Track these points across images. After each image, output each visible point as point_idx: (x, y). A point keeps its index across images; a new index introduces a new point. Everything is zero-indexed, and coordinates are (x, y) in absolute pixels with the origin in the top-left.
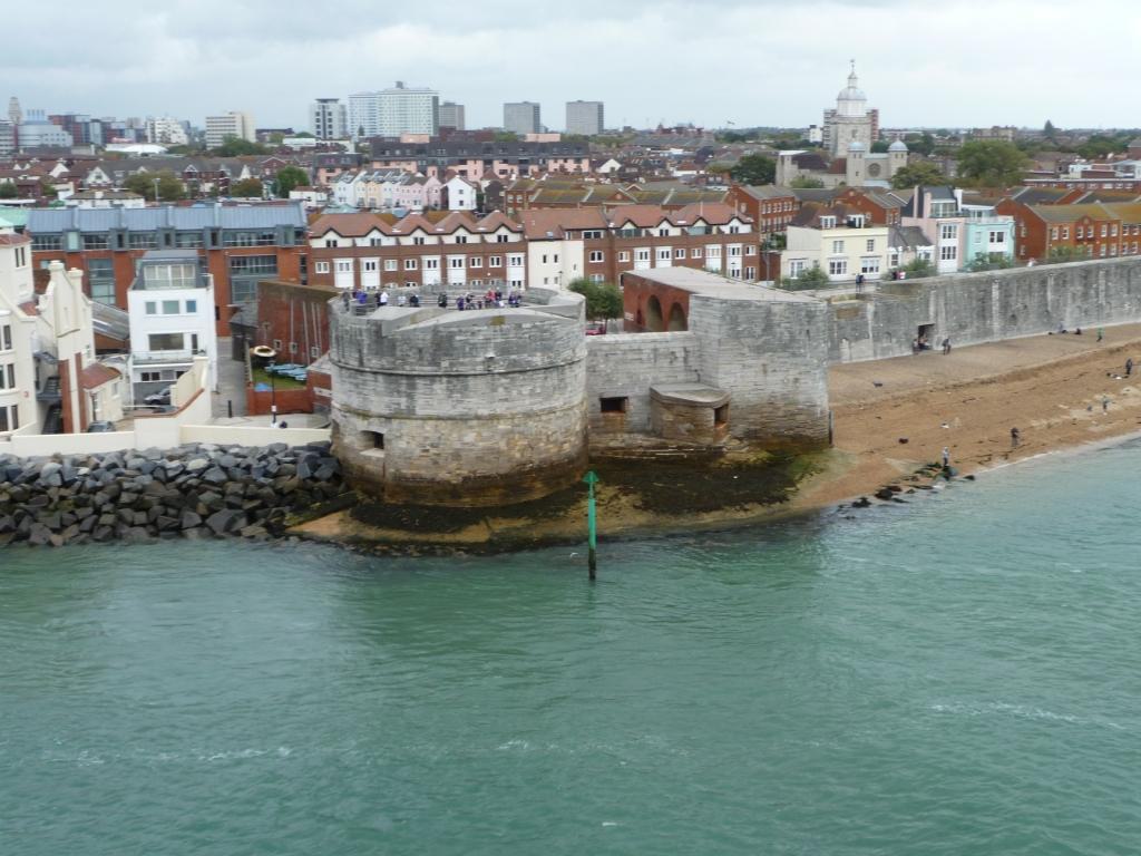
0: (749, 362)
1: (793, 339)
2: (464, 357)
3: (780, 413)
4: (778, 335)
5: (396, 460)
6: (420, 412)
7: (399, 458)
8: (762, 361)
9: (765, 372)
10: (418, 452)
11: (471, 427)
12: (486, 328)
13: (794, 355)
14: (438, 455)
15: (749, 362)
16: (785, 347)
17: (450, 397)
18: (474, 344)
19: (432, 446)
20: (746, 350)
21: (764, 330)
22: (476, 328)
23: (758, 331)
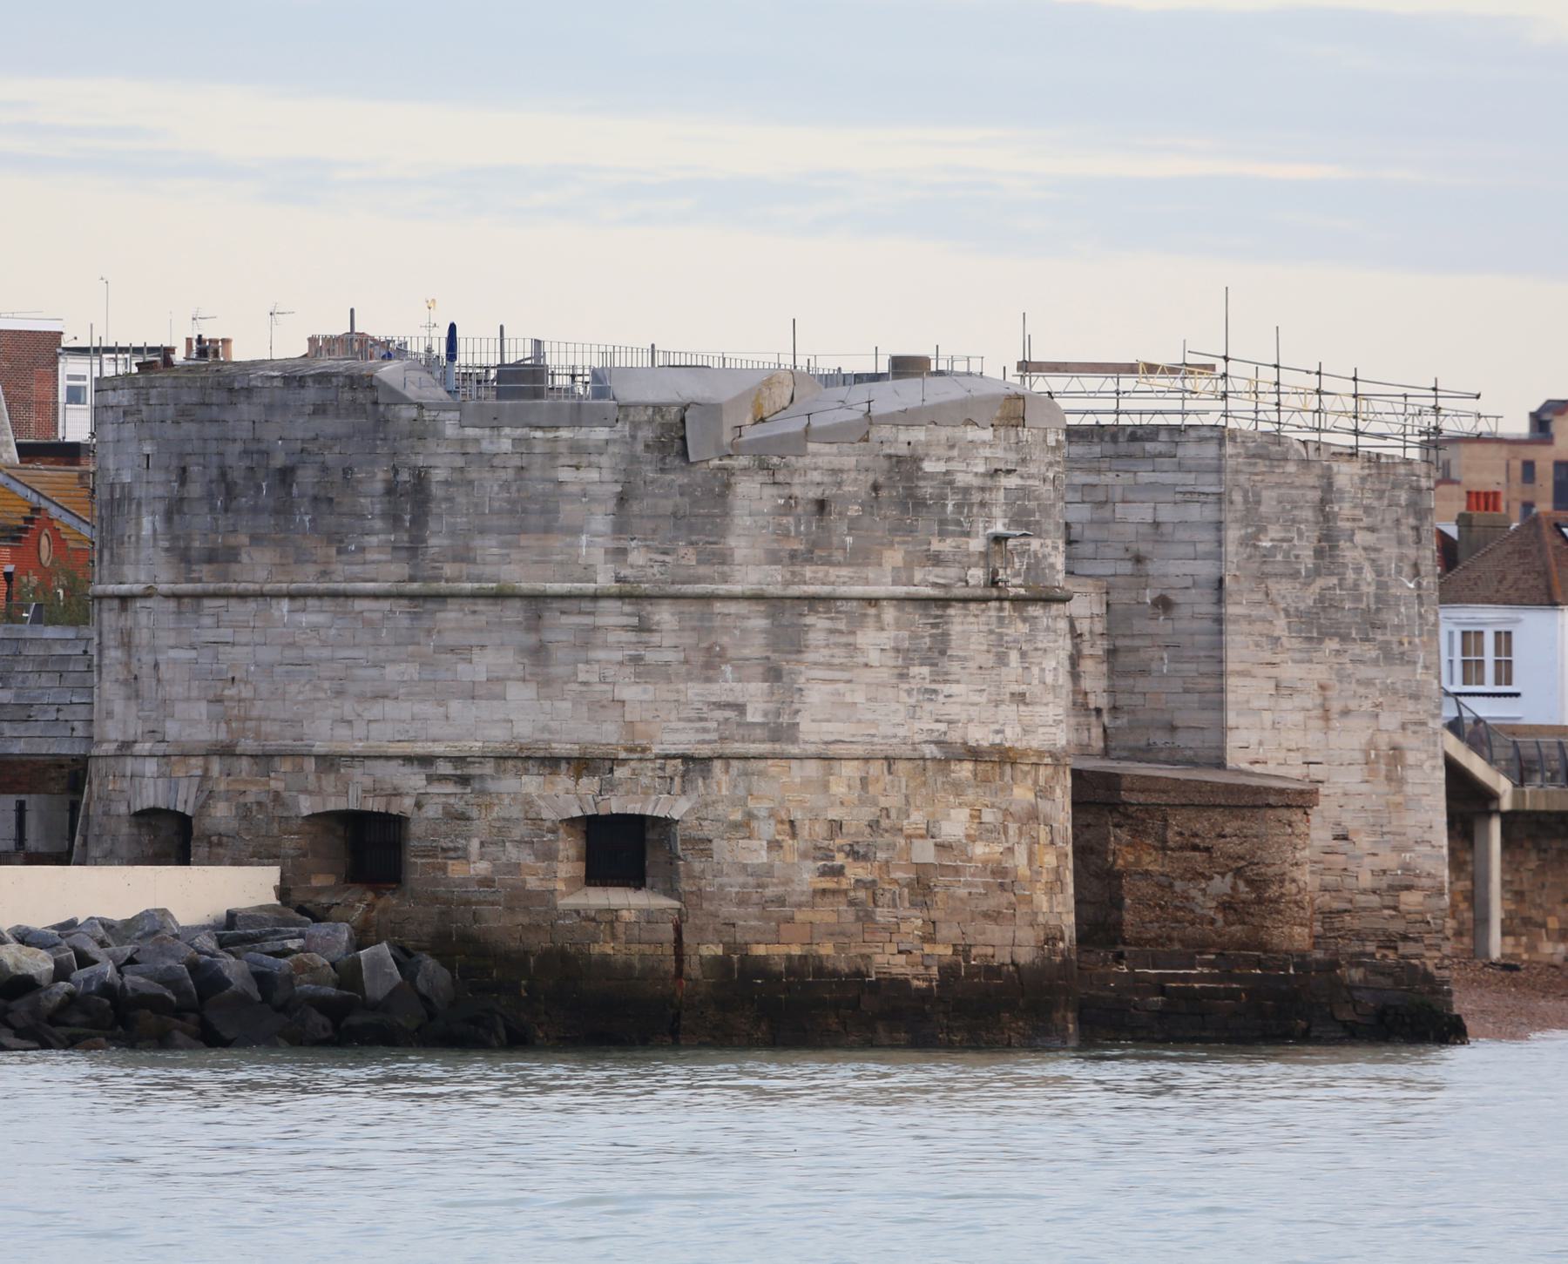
0: (1290, 672)
1: (1383, 599)
2: (943, 534)
3: (1366, 880)
4: (1350, 575)
5: (729, 910)
6: (813, 730)
7: (742, 901)
8: (1320, 673)
9: (1326, 716)
10: (807, 877)
11: (957, 788)
12: (987, 434)
13: (1388, 656)
14: (871, 886)
15: (1290, 672)
16: (1371, 623)
17: (903, 676)
18: (966, 490)
19: (853, 854)
20: (1281, 623)
21: (1319, 553)
22: (972, 433)
23: (1307, 560)
